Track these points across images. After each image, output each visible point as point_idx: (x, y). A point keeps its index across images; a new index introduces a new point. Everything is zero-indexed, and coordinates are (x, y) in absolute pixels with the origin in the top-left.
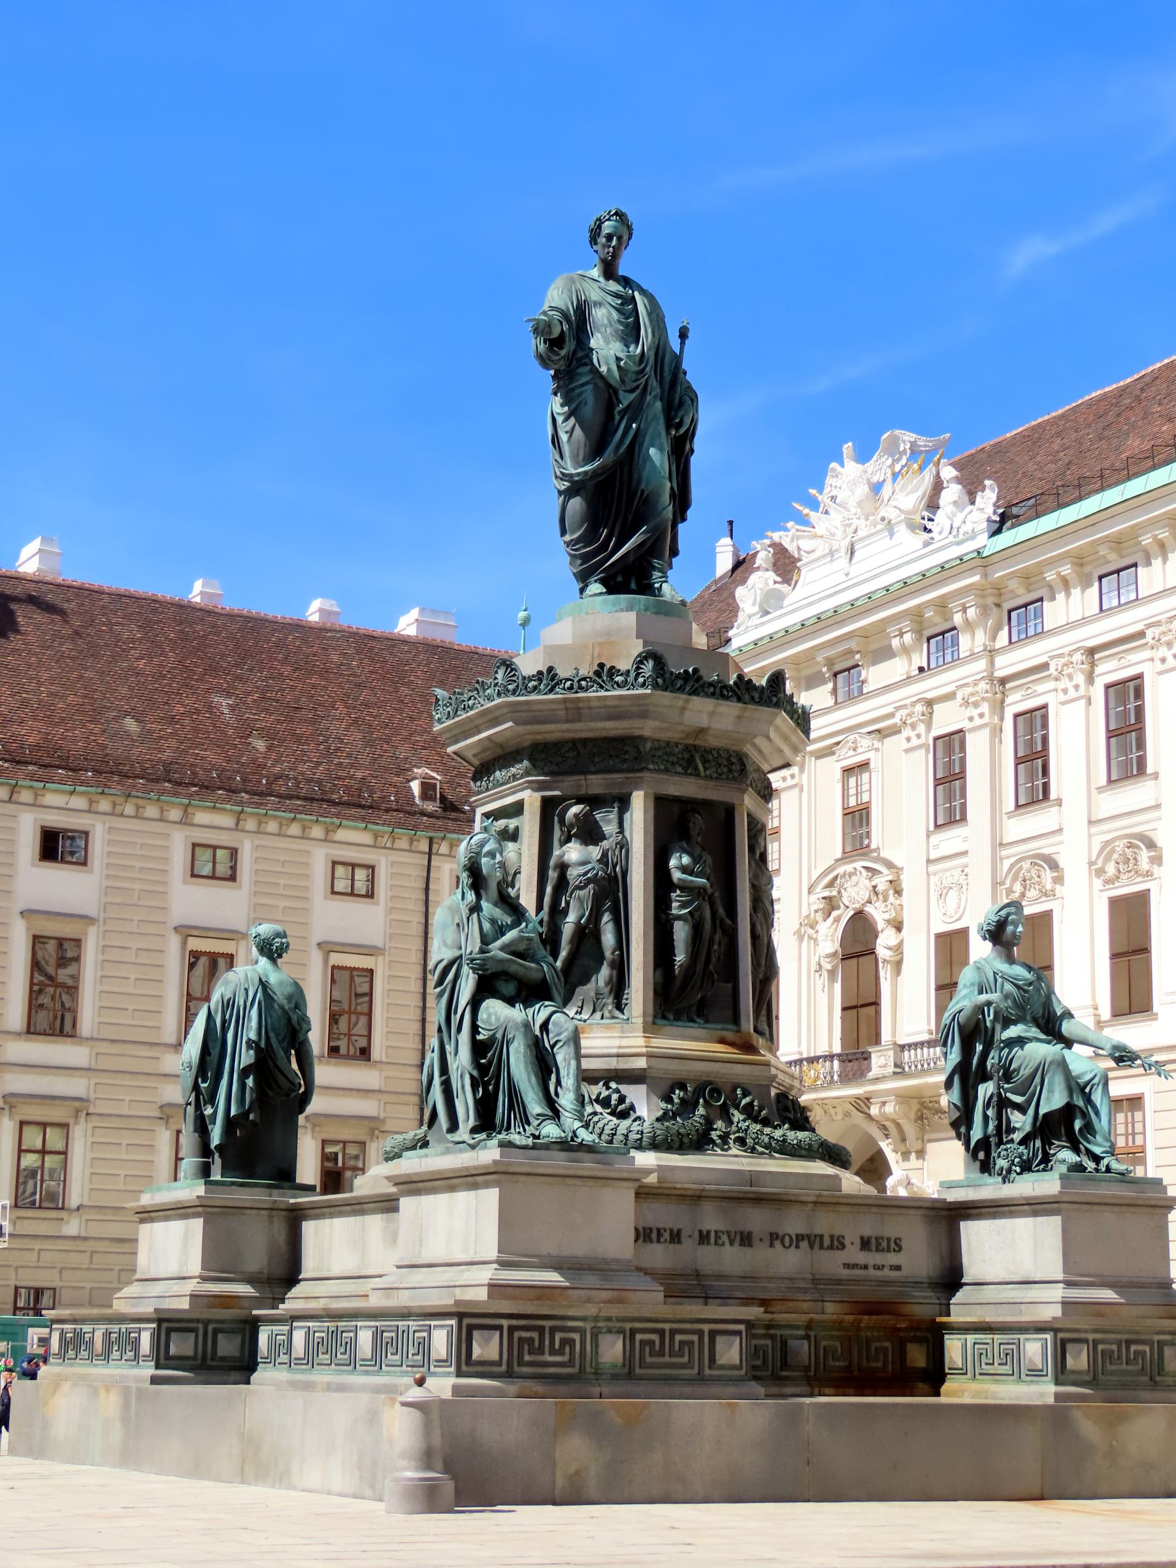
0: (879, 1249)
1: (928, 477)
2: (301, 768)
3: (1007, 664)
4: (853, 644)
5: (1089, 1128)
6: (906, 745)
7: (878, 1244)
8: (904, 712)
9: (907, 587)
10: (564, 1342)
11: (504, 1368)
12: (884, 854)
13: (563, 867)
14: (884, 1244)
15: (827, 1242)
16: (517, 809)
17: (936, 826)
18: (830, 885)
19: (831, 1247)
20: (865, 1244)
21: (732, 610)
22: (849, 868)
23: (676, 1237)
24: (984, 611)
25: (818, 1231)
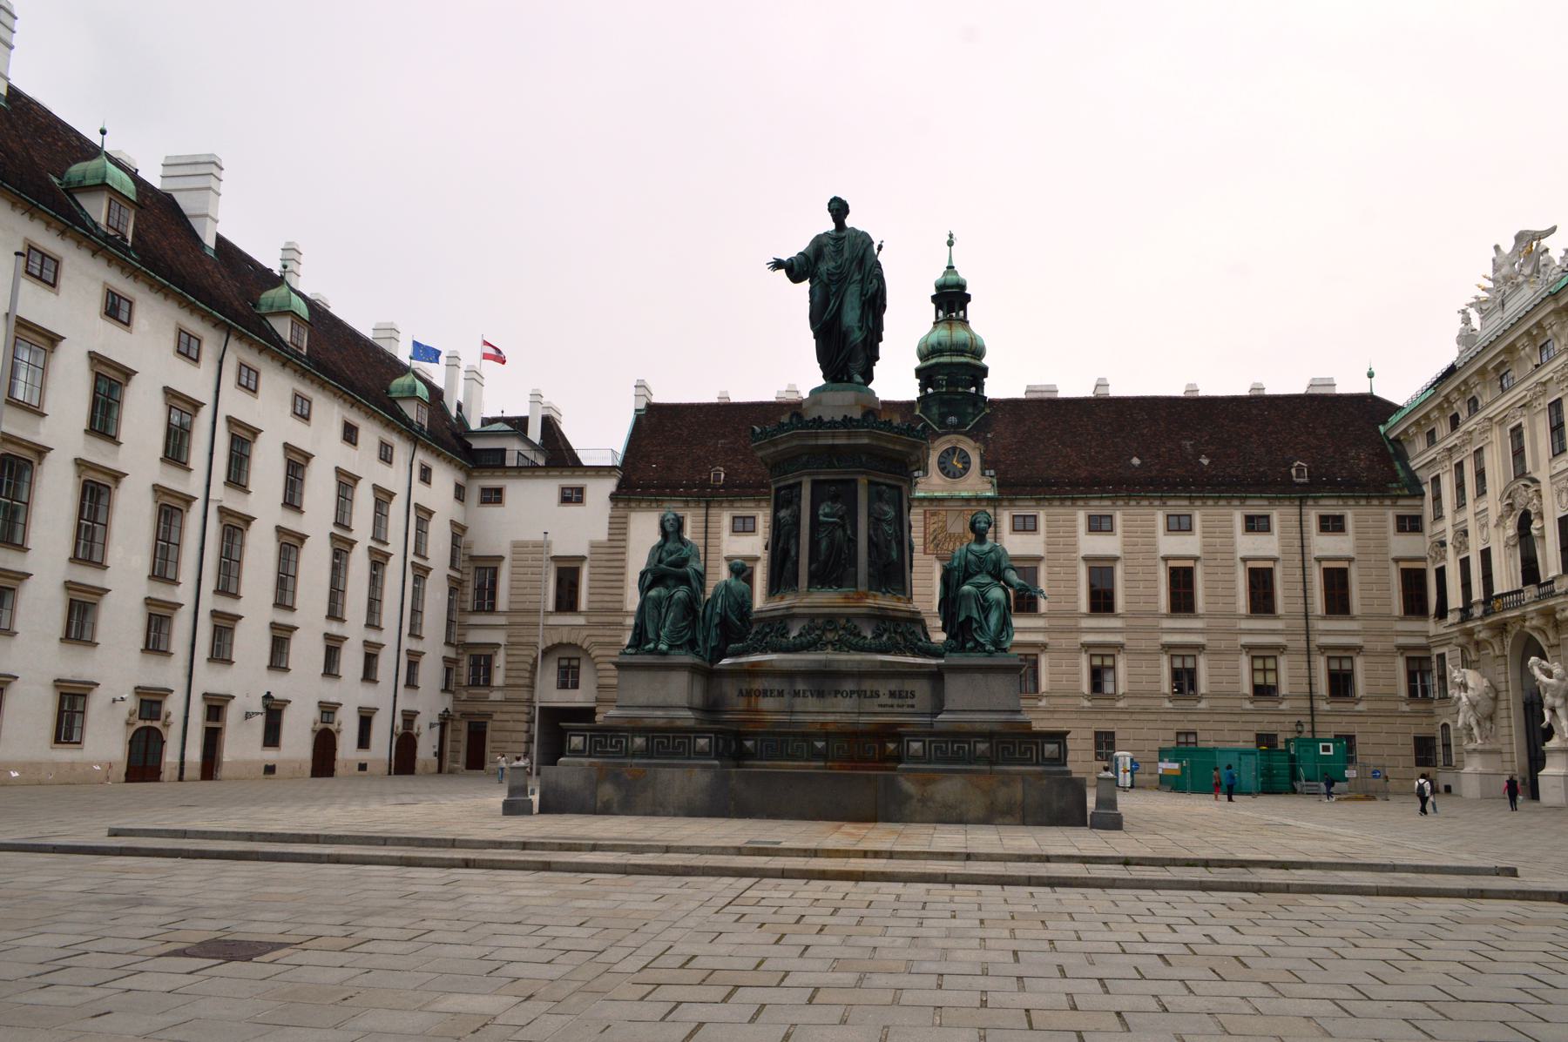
0: (900, 697)
2: (1228, 470)
5: (981, 627)
6: (1536, 410)
7: (900, 694)
8: (1531, 393)
10: (616, 742)
11: (587, 753)
12: (1534, 475)
14: (904, 694)
15: (868, 694)
17: (1554, 455)
18: (1509, 497)
19: (871, 697)
20: (892, 694)
22: (1515, 486)
23: (781, 694)
25: (863, 688)
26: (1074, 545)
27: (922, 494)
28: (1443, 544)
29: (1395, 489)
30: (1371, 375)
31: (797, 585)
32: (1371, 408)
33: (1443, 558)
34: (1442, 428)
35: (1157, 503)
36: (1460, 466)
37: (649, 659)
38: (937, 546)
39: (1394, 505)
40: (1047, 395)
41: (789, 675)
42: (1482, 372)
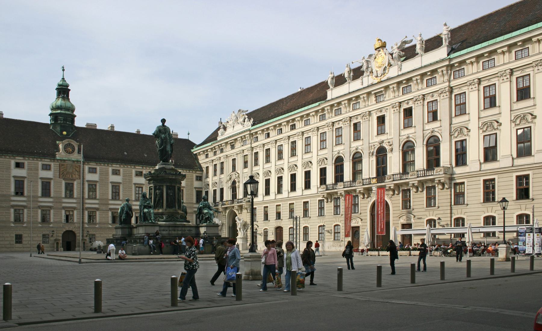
1: (244, 116)
3: (253, 145)
4: (233, 141)
9: (240, 133)
12: (237, 172)
13: (156, 193)
16: (152, 186)
18: (230, 176)
20: (188, 230)
21: (217, 135)
22: (232, 173)
23: (167, 230)
24: (250, 137)
26: (108, 179)
27: (59, 158)
28: (208, 185)
29: (196, 168)
30: (189, 134)
31: (163, 207)
32: (188, 144)
33: (208, 189)
34: (211, 154)
35: (133, 167)
36: (215, 165)
37: (150, 224)
38: (63, 175)
39: (195, 173)
40: (94, 128)
41: (169, 227)
42: (227, 143)
